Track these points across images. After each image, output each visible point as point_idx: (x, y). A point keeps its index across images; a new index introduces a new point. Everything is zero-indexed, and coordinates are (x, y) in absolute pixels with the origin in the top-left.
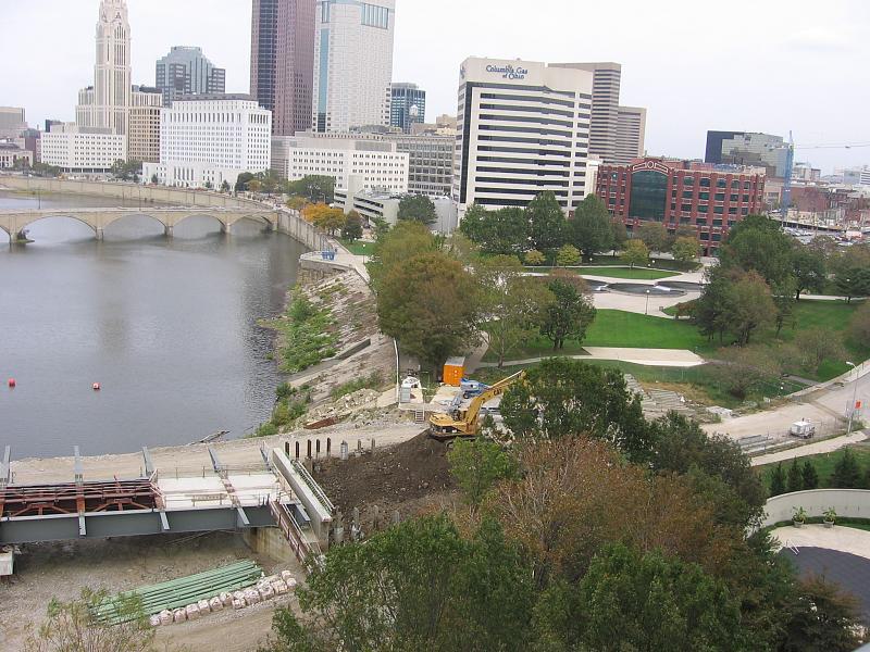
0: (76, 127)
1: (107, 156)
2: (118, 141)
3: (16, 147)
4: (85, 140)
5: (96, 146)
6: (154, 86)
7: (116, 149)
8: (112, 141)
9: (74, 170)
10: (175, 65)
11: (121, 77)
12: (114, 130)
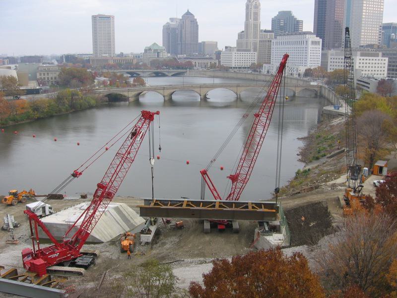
0: (235, 49)
1: (248, 62)
2: (253, 55)
3: (211, 58)
4: (239, 55)
5: (244, 57)
6: (270, 28)
7: (251, 58)
8: (251, 55)
9: (234, 68)
10: (280, 20)
11: (256, 26)
12: (252, 50)
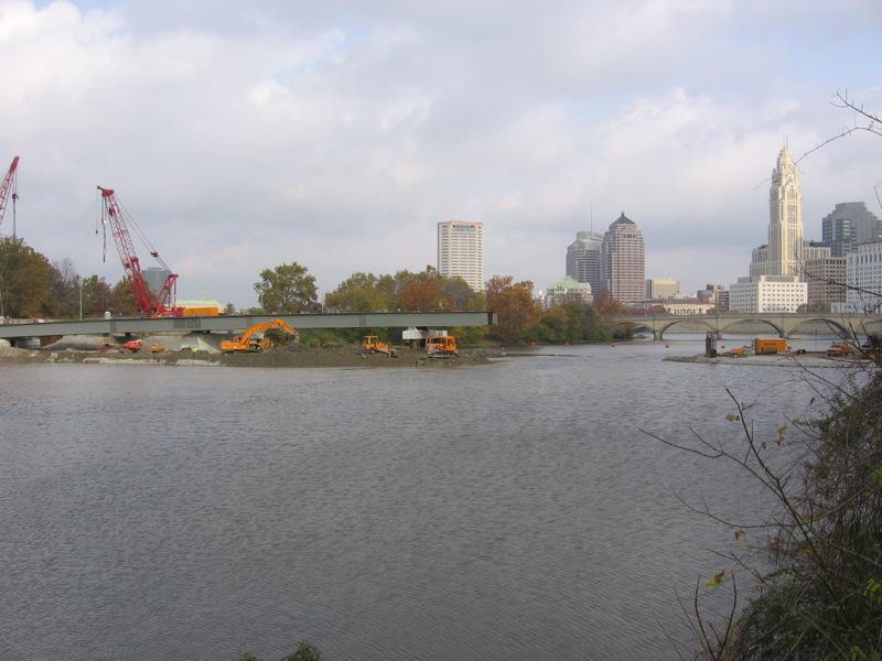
6: (819, 238)
